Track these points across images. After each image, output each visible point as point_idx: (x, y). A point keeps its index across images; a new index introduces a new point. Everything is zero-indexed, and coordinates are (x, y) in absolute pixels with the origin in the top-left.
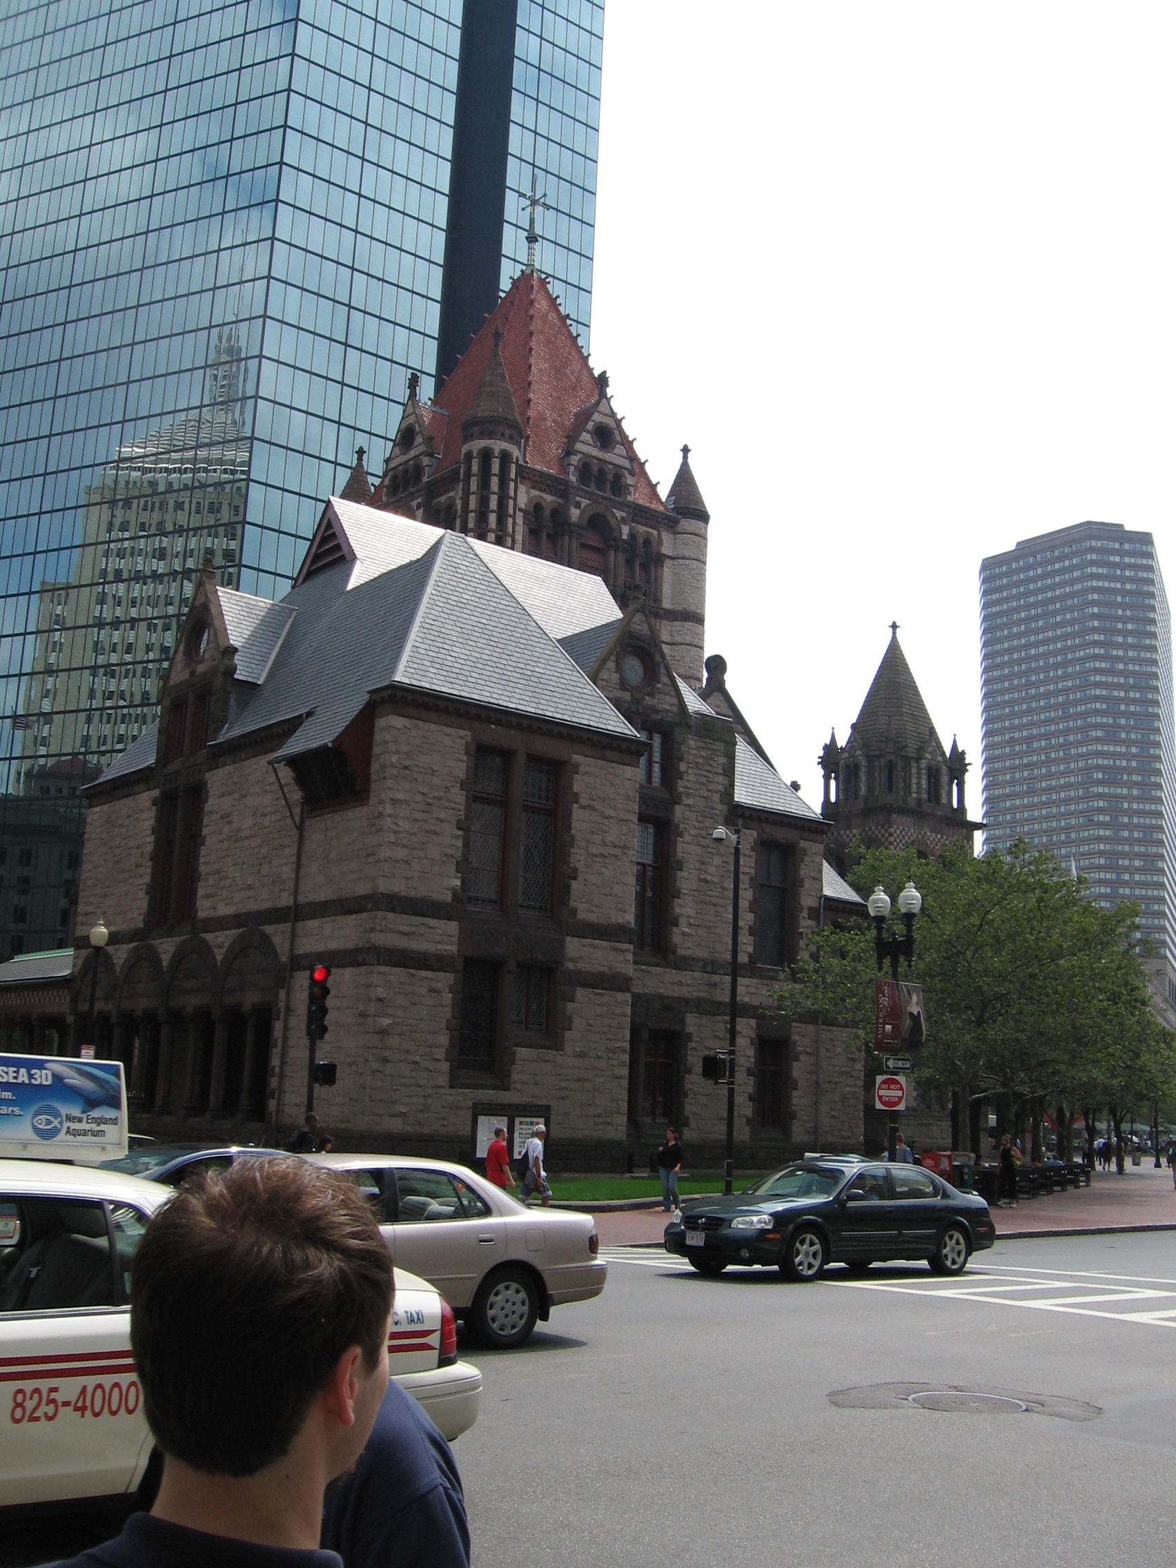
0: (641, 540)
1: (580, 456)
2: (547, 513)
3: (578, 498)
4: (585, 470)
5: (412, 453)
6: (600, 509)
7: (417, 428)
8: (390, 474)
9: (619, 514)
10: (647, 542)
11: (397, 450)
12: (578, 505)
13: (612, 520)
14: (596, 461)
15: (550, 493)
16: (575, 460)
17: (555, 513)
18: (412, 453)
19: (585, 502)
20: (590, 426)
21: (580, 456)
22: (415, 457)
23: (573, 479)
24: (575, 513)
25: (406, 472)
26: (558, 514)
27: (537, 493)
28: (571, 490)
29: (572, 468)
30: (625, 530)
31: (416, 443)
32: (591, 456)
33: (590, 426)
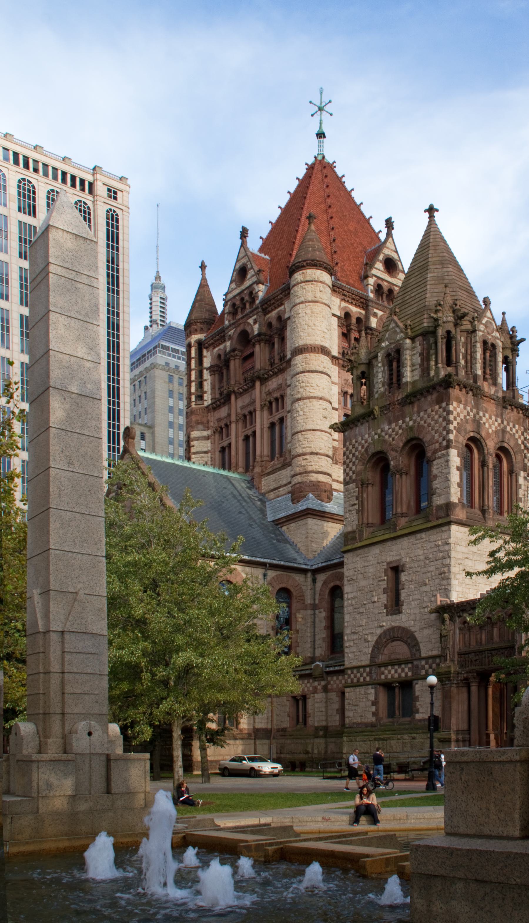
2: (354, 321)
3: (376, 311)
4: (379, 289)
5: (247, 283)
7: (249, 266)
8: (229, 303)
11: (233, 286)
12: (375, 315)
14: (386, 284)
15: (355, 305)
18: (247, 283)
19: (380, 313)
20: (381, 257)
22: (251, 285)
23: (371, 295)
25: (242, 299)
28: (370, 304)
29: (371, 288)
31: (249, 276)
32: (383, 280)
33: (381, 257)
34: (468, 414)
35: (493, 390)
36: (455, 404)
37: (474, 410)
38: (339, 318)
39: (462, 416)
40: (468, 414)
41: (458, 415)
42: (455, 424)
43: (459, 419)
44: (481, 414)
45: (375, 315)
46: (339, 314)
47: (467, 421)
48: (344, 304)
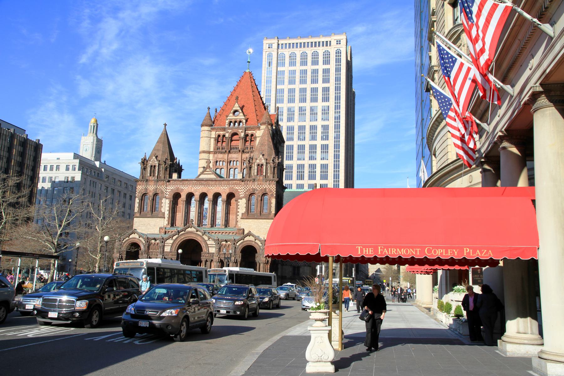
0: (250, 135)
1: (228, 120)
6: (235, 131)
9: (240, 131)
10: (252, 135)
12: (228, 132)
13: (238, 133)
16: (227, 121)
17: (224, 136)
19: (230, 131)
21: (228, 120)
24: (227, 135)
26: (224, 136)
27: (219, 132)
30: (242, 135)
32: (232, 119)
33: (232, 112)
34: (143, 187)
35: (153, 178)
36: (138, 186)
37: (145, 186)
38: (214, 138)
39: (141, 189)
40: (143, 187)
41: (139, 189)
42: (138, 191)
43: (139, 190)
44: (148, 186)
45: (228, 132)
46: (214, 137)
47: (142, 190)
48: (217, 133)
